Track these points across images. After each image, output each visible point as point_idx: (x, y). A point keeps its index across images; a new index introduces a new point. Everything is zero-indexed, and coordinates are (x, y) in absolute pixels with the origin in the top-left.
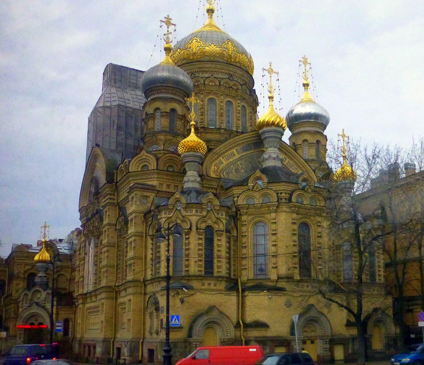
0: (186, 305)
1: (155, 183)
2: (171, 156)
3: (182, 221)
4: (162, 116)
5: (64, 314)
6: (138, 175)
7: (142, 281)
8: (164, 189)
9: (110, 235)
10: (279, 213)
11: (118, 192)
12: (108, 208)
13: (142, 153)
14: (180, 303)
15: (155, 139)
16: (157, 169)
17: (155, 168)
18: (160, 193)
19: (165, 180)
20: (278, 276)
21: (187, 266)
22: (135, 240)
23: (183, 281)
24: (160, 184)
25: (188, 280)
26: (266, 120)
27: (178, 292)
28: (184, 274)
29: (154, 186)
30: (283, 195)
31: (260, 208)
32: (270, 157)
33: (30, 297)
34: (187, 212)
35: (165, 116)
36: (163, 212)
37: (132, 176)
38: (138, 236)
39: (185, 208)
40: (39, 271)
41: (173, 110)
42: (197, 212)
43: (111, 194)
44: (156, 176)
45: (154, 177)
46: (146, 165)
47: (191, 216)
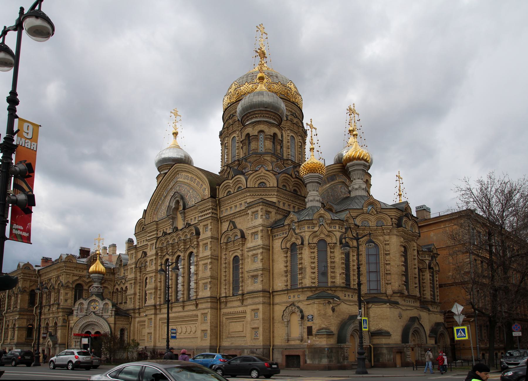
0: (336, 313)
1: (274, 200)
5: (121, 324)
6: (256, 191)
8: (281, 206)
11: (220, 207)
12: (210, 221)
13: (260, 171)
14: (332, 312)
16: (277, 187)
17: (276, 185)
18: (280, 210)
21: (333, 277)
22: (262, 253)
23: (329, 292)
24: (279, 202)
27: (329, 302)
28: (329, 285)
33: (85, 306)
34: (331, 228)
37: (249, 192)
38: (265, 249)
39: (329, 224)
40: (95, 282)
43: (213, 209)
45: (274, 195)
46: (263, 182)
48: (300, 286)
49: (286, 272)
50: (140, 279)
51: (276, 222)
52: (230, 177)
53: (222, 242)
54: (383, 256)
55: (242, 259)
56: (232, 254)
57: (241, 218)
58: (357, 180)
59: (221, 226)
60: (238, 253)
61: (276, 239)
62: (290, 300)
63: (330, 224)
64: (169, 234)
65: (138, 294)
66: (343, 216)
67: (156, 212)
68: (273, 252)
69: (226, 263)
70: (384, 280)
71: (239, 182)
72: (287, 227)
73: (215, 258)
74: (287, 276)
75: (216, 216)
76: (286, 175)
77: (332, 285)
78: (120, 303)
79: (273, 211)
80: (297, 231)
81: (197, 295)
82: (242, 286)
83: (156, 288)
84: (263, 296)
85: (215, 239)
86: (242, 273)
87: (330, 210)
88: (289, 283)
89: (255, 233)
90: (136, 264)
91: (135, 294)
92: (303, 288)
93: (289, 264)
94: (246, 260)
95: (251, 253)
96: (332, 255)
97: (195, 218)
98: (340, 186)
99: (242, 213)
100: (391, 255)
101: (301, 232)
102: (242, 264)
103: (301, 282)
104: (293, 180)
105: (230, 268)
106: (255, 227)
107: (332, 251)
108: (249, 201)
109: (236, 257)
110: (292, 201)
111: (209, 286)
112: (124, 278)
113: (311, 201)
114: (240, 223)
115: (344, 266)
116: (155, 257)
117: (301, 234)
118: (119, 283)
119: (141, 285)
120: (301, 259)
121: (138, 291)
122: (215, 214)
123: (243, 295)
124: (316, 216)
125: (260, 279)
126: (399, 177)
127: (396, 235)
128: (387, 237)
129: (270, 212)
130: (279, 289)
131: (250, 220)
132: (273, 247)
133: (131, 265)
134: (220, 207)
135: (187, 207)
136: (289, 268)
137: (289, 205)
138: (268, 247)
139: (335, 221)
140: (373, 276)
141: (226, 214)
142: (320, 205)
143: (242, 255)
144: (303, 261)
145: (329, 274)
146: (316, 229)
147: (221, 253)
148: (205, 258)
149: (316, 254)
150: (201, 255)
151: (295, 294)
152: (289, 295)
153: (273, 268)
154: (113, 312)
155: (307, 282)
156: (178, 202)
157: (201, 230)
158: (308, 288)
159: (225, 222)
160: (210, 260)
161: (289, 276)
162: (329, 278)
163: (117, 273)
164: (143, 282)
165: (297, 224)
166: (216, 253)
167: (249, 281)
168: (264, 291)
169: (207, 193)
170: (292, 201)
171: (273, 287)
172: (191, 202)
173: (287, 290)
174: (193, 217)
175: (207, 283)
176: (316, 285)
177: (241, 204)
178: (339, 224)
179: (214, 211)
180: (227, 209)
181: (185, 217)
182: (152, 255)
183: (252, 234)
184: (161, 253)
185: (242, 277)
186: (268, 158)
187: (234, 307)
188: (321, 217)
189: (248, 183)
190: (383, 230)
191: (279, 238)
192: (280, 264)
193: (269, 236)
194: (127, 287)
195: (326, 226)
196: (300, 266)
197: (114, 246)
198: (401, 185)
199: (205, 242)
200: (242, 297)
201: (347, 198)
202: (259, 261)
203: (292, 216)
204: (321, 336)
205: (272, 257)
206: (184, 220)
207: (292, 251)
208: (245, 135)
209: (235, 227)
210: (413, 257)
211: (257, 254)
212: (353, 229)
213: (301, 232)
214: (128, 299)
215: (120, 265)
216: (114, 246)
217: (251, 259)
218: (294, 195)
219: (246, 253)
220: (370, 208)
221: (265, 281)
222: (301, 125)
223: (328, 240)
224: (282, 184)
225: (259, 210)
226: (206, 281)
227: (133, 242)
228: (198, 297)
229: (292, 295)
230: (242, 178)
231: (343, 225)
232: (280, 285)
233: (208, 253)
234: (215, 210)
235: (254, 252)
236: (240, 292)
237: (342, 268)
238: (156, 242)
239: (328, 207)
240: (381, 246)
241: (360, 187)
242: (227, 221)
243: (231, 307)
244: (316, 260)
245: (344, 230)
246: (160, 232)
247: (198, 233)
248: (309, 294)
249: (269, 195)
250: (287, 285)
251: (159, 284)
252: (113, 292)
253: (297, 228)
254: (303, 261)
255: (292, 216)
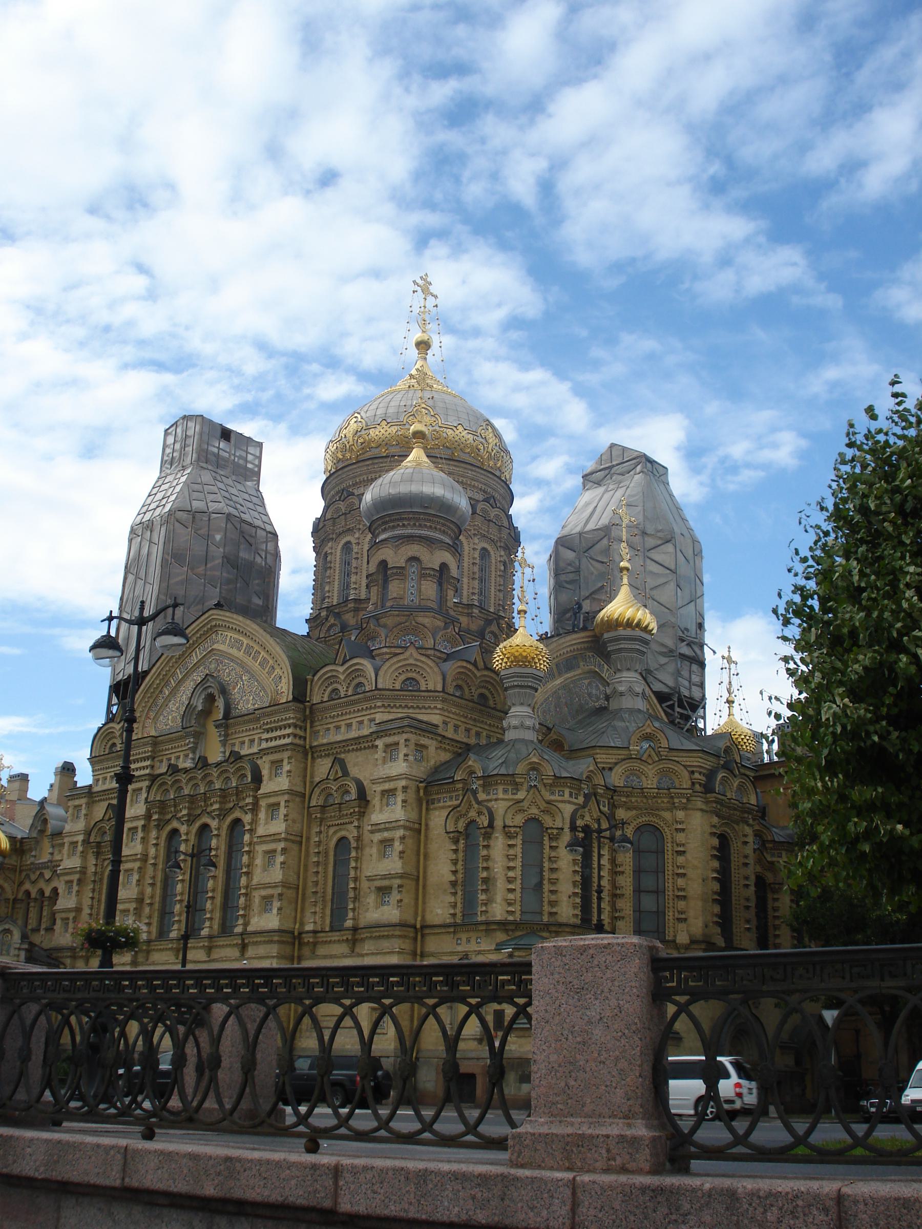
1: (436, 719)
2: (466, 668)
3: (543, 811)
4: (423, 576)
6: (396, 698)
7: (418, 926)
8: (450, 734)
9: (291, 817)
10: (691, 812)
11: (312, 723)
12: (286, 755)
13: (407, 654)
15: (413, 623)
16: (443, 691)
17: (439, 688)
19: (451, 716)
20: (690, 936)
22: (403, 838)
24: (445, 723)
25: (556, 932)
26: (616, 616)
28: (545, 919)
29: (437, 726)
30: (697, 775)
31: (655, 797)
32: (615, 691)
34: (553, 793)
35: (430, 575)
36: (500, 788)
37: (382, 698)
41: (444, 567)
42: (571, 795)
43: (296, 726)
44: (439, 706)
45: (435, 708)
46: (413, 679)
47: (562, 802)
48: (483, 918)
49: (454, 884)
50: (96, 873)
51: (436, 770)
52: (340, 660)
53: (313, 803)
54: (670, 857)
55: (357, 848)
56: (335, 832)
57: (358, 753)
58: (625, 674)
59: (313, 766)
60: (350, 833)
61: (435, 809)
62: (460, 949)
63: (551, 785)
64: (186, 771)
65: (86, 911)
66: (582, 767)
67: (152, 715)
68: (426, 836)
69: (319, 853)
70: (671, 910)
71: (358, 672)
72: (461, 785)
73: (296, 840)
74: (455, 894)
75: (301, 742)
76: (465, 664)
77: (552, 920)
78: (33, 930)
79: (432, 744)
80: (482, 796)
81: (246, 924)
82: (354, 910)
83: (140, 901)
84: (400, 936)
85: (299, 796)
86: (356, 879)
87: (557, 746)
88: (458, 911)
89: (391, 793)
90: (88, 833)
91: (78, 910)
92: (487, 923)
93: (460, 866)
94: (367, 851)
95: (377, 837)
96: (553, 854)
97: (252, 741)
98: (586, 682)
99: (363, 744)
100: (688, 855)
101: (490, 800)
102: (357, 859)
103: (484, 908)
104: (478, 674)
105: (326, 865)
106: (389, 779)
107: (554, 844)
108: (379, 717)
109: (343, 838)
110: (475, 720)
111: (276, 904)
112: (53, 866)
113: (515, 728)
114: (355, 765)
115: (578, 878)
116: (142, 822)
117: (489, 805)
118: (33, 877)
119: (97, 887)
120: (487, 858)
121: (87, 902)
122: (300, 737)
123: (355, 929)
124: (521, 769)
125: (395, 896)
126: (730, 660)
127: (702, 810)
128: (680, 814)
129: (425, 747)
130: (437, 921)
131: (380, 762)
132: (427, 825)
133: (71, 834)
134: (312, 723)
135: (234, 713)
136: (460, 876)
137: (468, 730)
138: (417, 826)
139: (562, 781)
140: (649, 903)
141: (325, 741)
142: (531, 736)
143: (358, 839)
144: (490, 864)
145: (546, 895)
146: (521, 795)
147: (309, 827)
148: (274, 838)
149: (519, 850)
150: (261, 831)
151: (471, 934)
152: (458, 936)
153: (425, 872)
154: (23, 954)
155: (498, 911)
156: (211, 699)
157: (265, 772)
158: (499, 923)
159: (321, 757)
160: (282, 845)
161: (460, 893)
162: (545, 904)
163: (31, 850)
164: (101, 880)
165: (481, 782)
166: (297, 828)
167: (371, 899)
168: (402, 925)
169: (285, 689)
170: (475, 720)
171: (423, 917)
172: (246, 703)
173: (455, 925)
174: (246, 739)
175: (272, 896)
176: (518, 917)
177: (361, 722)
178: (570, 787)
179: (298, 732)
180: (328, 729)
181: (226, 735)
182: (136, 818)
183: (384, 792)
184: (160, 813)
185: (355, 889)
186: (426, 621)
187: (332, 957)
188: (533, 769)
189: (380, 680)
190: (672, 797)
191: (443, 808)
192: (442, 866)
193: (419, 801)
194: (55, 890)
195: (543, 792)
196: (485, 874)
197: (23, 779)
198: (734, 679)
199: (272, 800)
200: (354, 935)
201: (601, 711)
202: (395, 855)
203: (470, 763)
204: (521, 1033)
205: (425, 848)
206: (224, 745)
207: (467, 837)
208: (377, 562)
209: (346, 773)
210: (743, 860)
211: (392, 840)
212: (602, 796)
213: (490, 800)
214: (58, 922)
215: (42, 832)
216: (23, 779)
217: (379, 851)
218: (479, 707)
219: (366, 832)
220: (646, 745)
221: (406, 901)
222: (506, 524)
223: (547, 821)
224: (454, 684)
225: (402, 741)
226: (269, 892)
227: (74, 770)
228: (249, 929)
229: (464, 937)
230: (367, 665)
231: (580, 789)
232: (439, 911)
233: (278, 826)
234: (301, 728)
235: (386, 834)
236: (349, 923)
237: (574, 883)
238: (149, 788)
239: (553, 736)
240: (667, 832)
241: (630, 690)
242: (328, 755)
243: (325, 957)
244: (518, 863)
245: (581, 800)
246: (161, 761)
247: (257, 779)
248: (501, 936)
249: (424, 707)
250: (454, 915)
251: (149, 890)
252: (15, 900)
253: (480, 789)
254: (490, 864)
255: (470, 763)
